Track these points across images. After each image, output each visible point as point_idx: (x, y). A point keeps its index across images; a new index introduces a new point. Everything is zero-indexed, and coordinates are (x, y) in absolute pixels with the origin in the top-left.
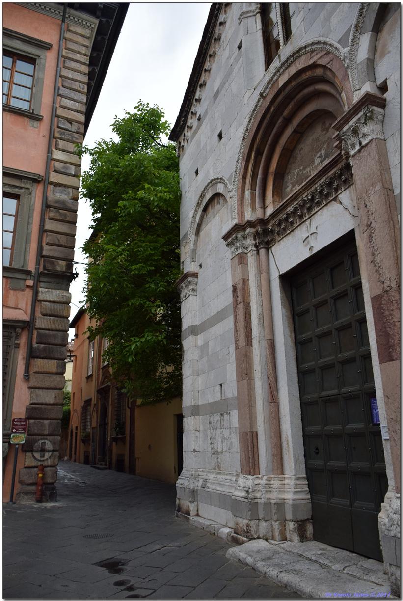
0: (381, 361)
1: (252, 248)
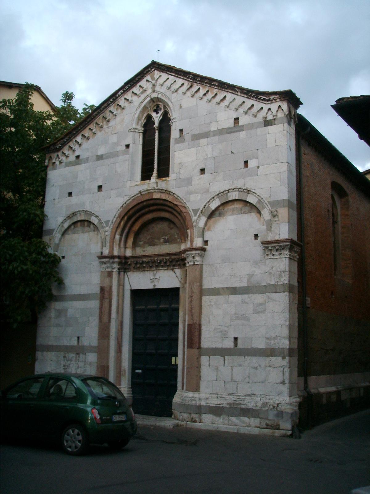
0: (188, 348)
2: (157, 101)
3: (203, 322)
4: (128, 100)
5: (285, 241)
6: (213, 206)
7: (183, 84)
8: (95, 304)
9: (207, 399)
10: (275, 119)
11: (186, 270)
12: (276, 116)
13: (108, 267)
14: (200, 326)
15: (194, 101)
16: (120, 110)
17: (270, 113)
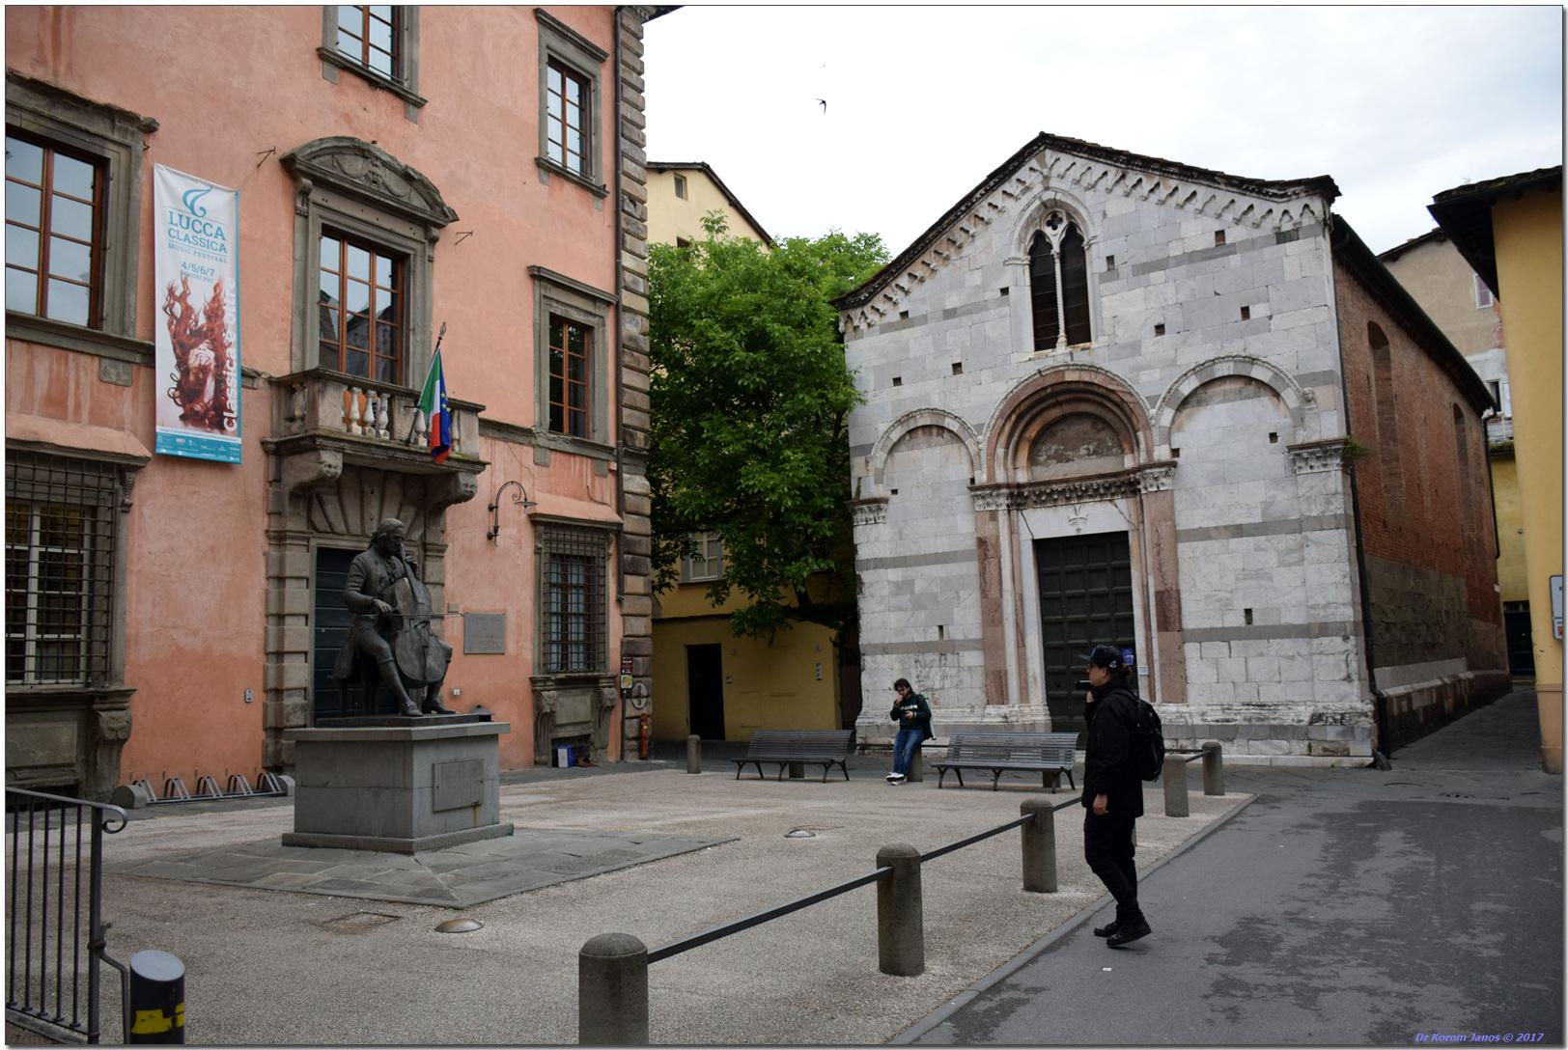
1: (1004, 507)
2: (1052, 207)
3: (1183, 586)
4: (996, 207)
5: (1336, 442)
6: (1186, 389)
7: (1105, 173)
8: (971, 568)
9: (1203, 714)
10: (1297, 230)
11: (1141, 501)
12: (1300, 223)
13: (988, 504)
14: (1178, 592)
15: (1129, 204)
16: (980, 226)
17: (1286, 218)
